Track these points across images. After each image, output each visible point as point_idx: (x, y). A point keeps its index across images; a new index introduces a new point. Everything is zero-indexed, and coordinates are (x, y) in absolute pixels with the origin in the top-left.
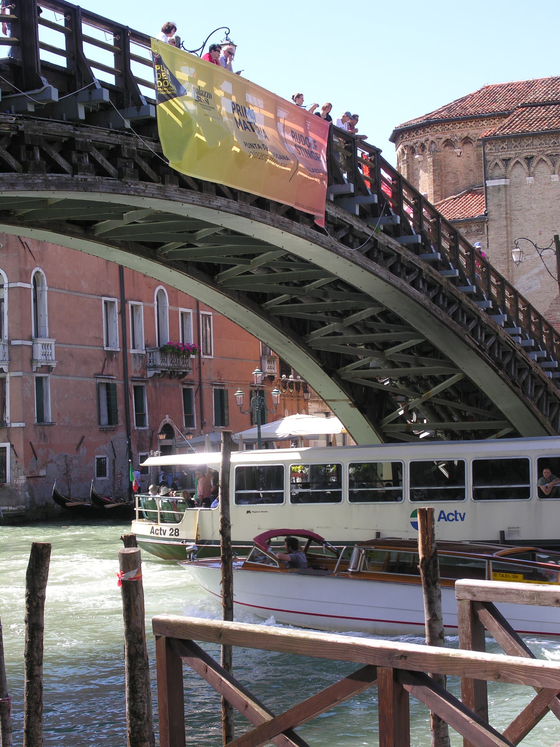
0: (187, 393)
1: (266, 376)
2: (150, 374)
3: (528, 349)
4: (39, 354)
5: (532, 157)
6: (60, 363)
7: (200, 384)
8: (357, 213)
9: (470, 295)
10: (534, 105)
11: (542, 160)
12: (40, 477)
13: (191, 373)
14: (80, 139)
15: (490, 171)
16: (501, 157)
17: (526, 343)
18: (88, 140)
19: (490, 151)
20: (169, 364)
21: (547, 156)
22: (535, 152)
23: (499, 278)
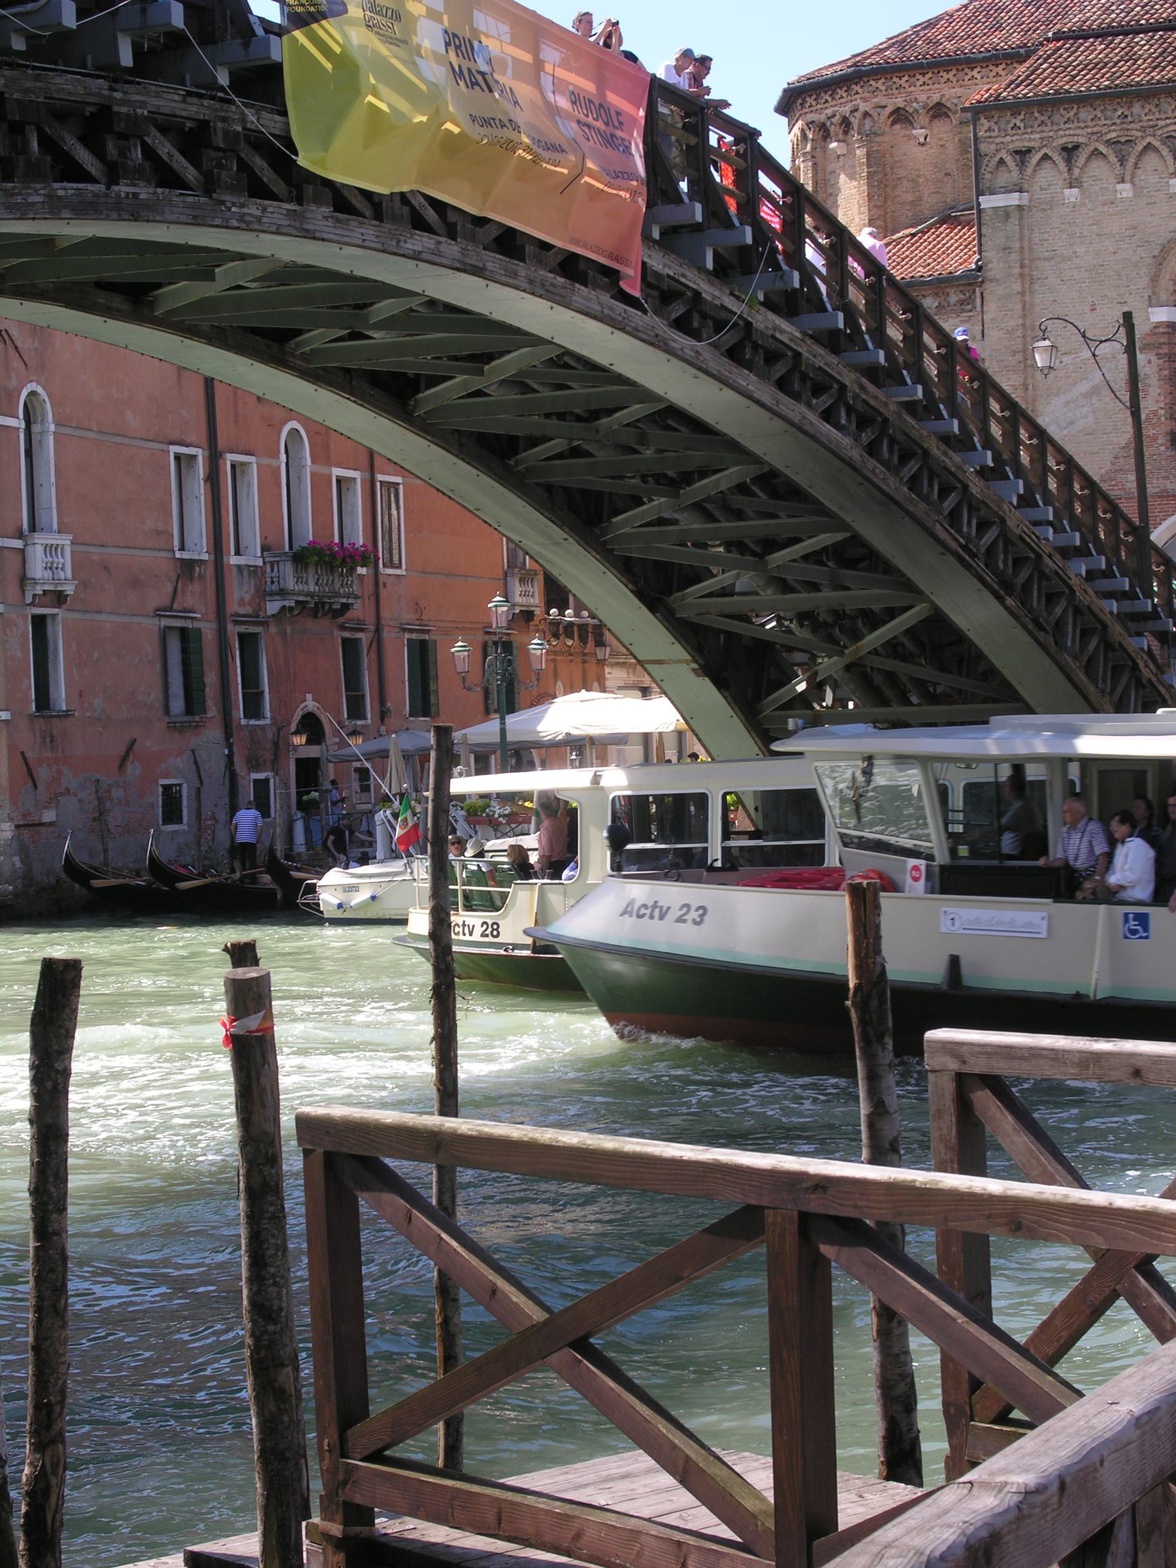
0: (350, 648)
1: (517, 611)
2: (273, 607)
3: (1067, 553)
4: (37, 567)
5: (1076, 147)
6: (83, 585)
7: (378, 630)
8: (710, 265)
9: (946, 439)
10: (1080, 35)
11: (1096, 153)
12: (44, 824)
13: (358, 604)
14: (124, 110)
15: (988, 176)
16: (1011, 146)
17: (1062, 540)
18: (139, 111)
19: (987, 134)
20: (312, 587)
21: (1109, 143)
22: (1083, 136)
23: (1007, 402)
